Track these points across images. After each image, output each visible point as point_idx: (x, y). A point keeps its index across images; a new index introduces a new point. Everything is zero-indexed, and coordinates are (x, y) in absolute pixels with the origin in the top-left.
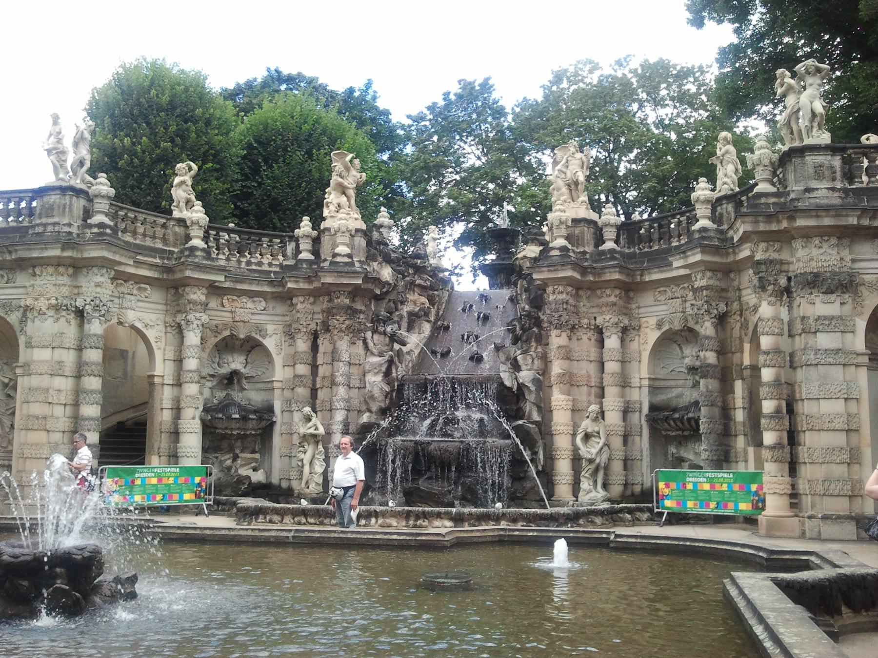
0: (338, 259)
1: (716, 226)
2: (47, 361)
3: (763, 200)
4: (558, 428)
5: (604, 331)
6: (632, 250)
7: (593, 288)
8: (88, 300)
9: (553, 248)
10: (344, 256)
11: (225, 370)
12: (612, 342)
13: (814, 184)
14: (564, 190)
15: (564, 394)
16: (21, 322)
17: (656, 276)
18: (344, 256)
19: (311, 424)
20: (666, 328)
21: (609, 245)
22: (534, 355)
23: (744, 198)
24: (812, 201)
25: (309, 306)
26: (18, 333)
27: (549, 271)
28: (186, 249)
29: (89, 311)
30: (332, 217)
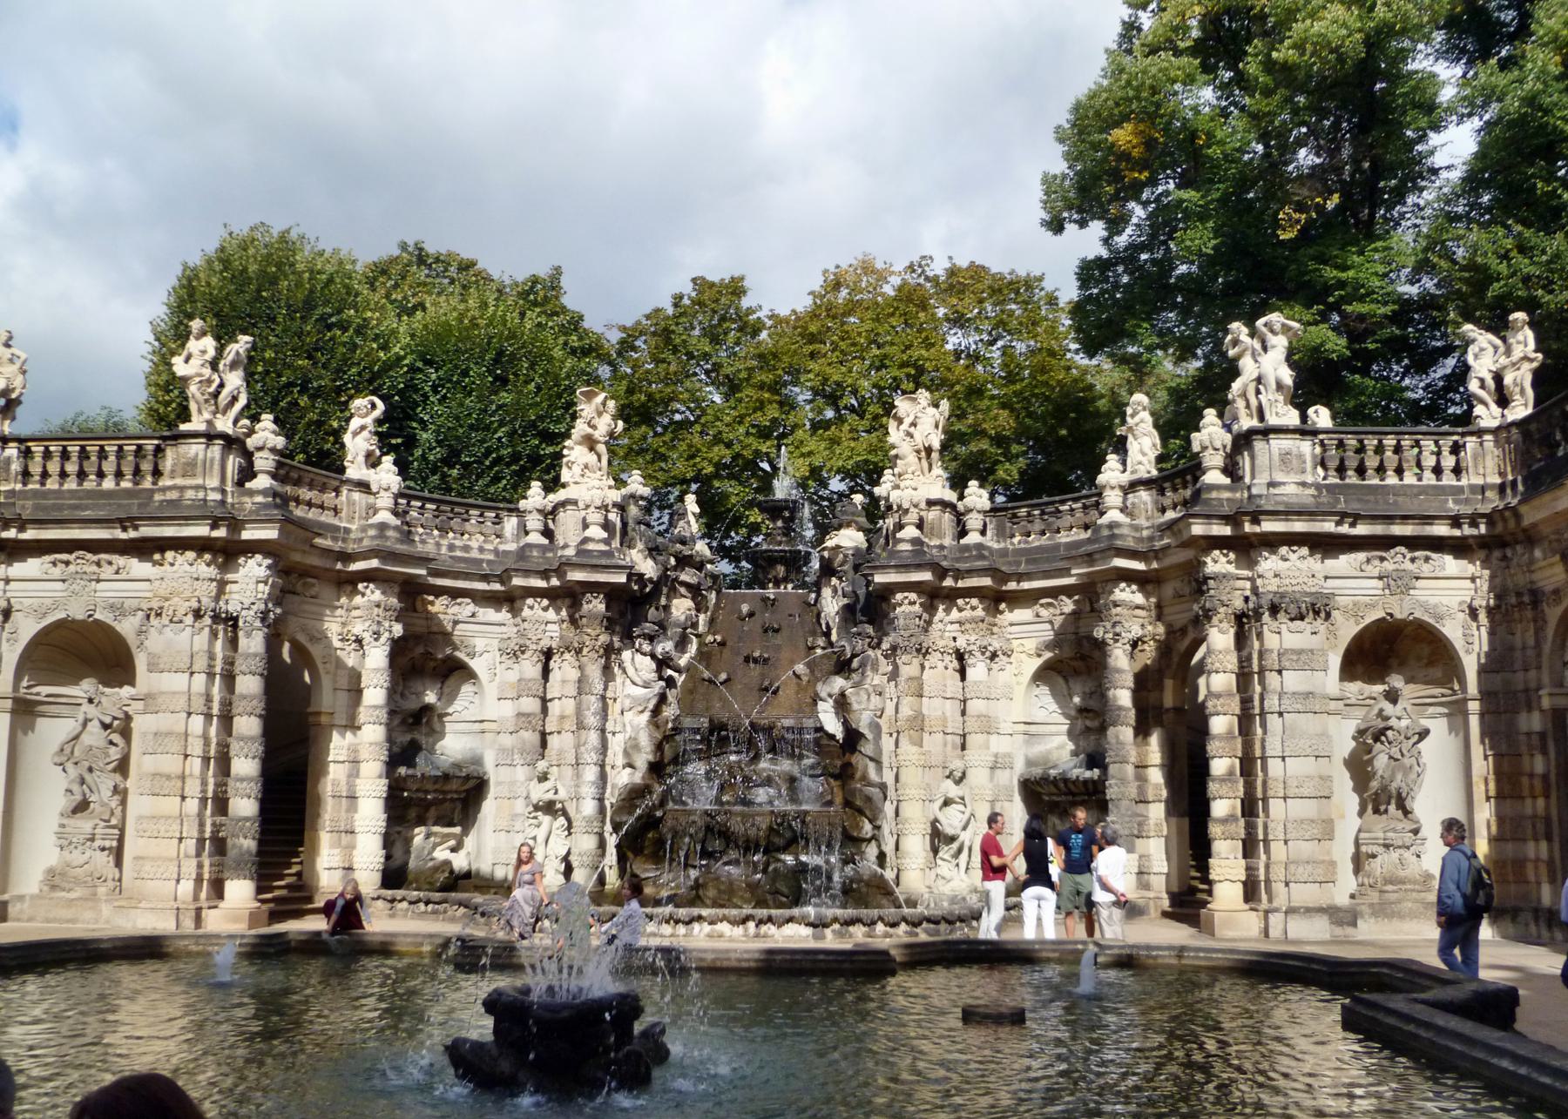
0: (591, 546)
1: (1128, 520)
3: (1214, 495)
6: (1002, 545)
7: (951, 596)
9: (902, 540)
10: (599, 541)
11: (412, 705)
12: (977, 670)
13: (1279, 477)
14: (912, 458)
18: (599, 541)
19: (547, 785)
21: (973, 538)
23: (1167, 485)
24: (1278, 499)
28: (371, 526)
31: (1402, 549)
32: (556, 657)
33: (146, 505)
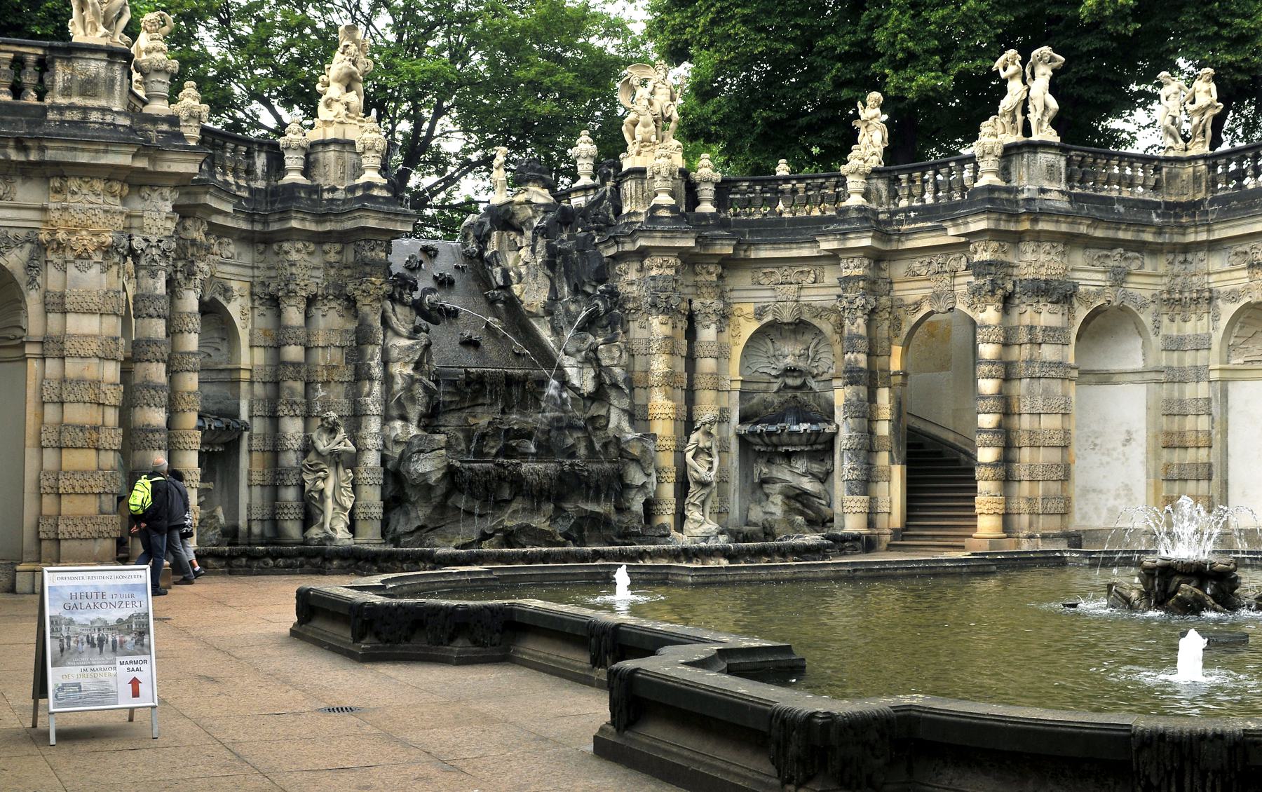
0: (376, 192)
2: (95, 336)
4: (664, 443)
5: (699, 318)
8: (154, 240)
12: (707, 334)
13: (1047, 185)
15: (668, 398)
16: (29, 267)
17: (764, 254)
20: (768, 318)
22: (622, 346)
25: (306, 257)
26: (23, 287)
27: (662, 237)
29: (157, 257)
30: (342, 123)
31: (1121, 250)
32: (319, 304)
33: (40, 124)
